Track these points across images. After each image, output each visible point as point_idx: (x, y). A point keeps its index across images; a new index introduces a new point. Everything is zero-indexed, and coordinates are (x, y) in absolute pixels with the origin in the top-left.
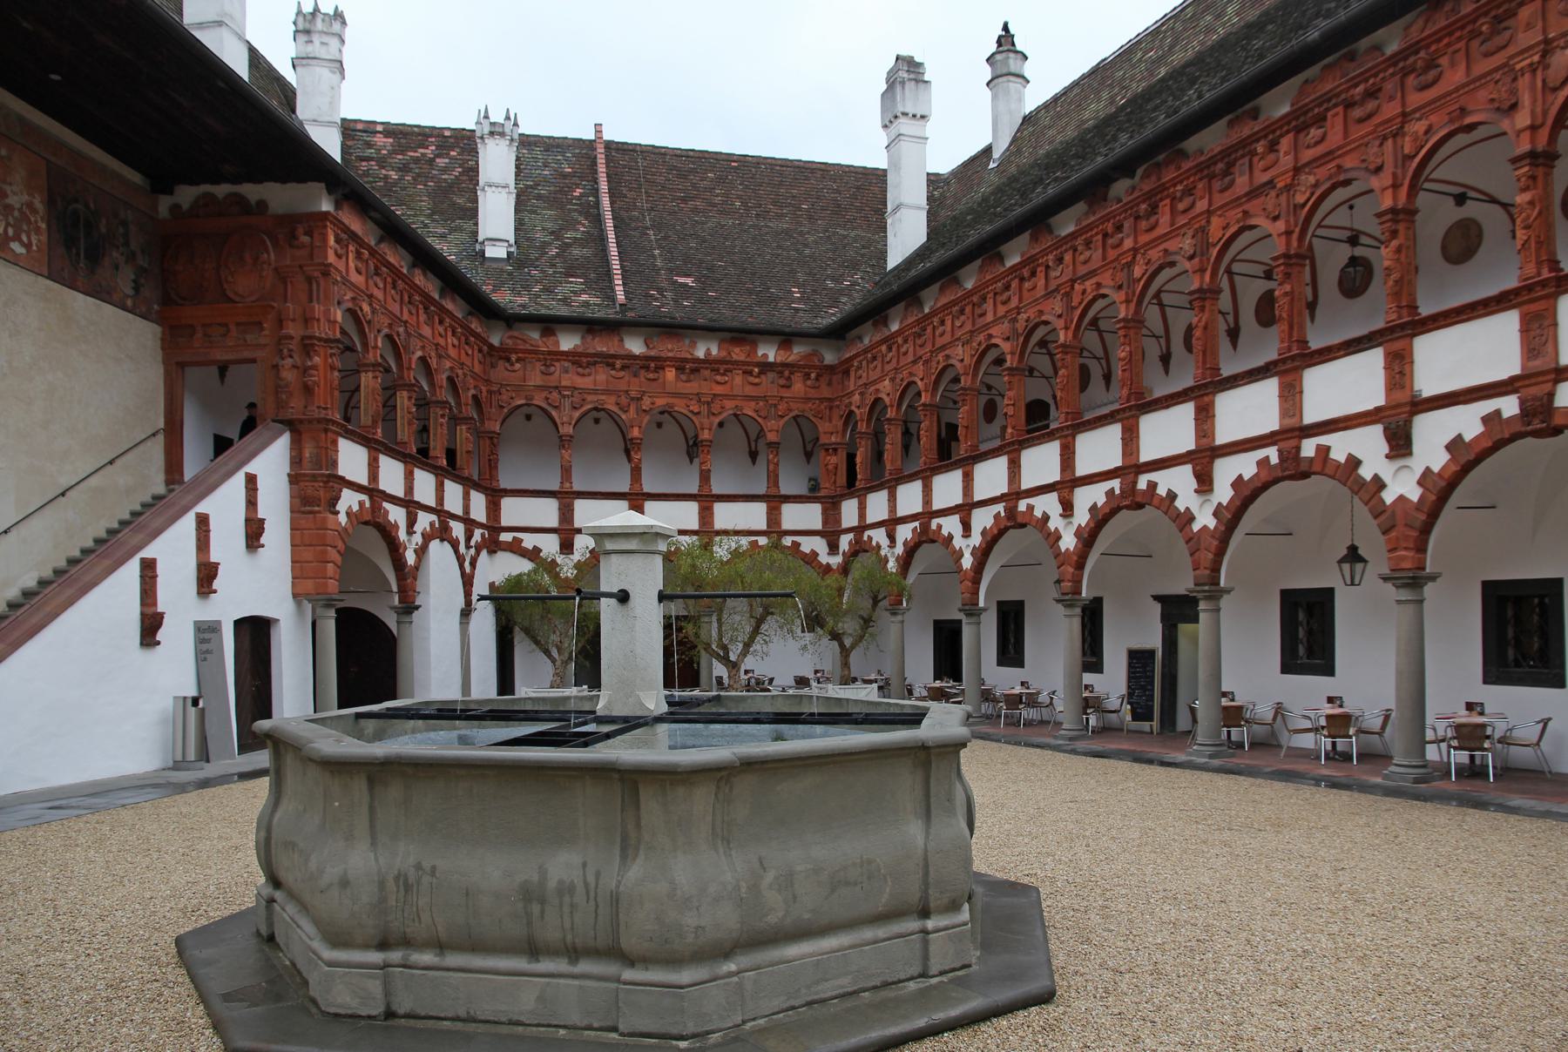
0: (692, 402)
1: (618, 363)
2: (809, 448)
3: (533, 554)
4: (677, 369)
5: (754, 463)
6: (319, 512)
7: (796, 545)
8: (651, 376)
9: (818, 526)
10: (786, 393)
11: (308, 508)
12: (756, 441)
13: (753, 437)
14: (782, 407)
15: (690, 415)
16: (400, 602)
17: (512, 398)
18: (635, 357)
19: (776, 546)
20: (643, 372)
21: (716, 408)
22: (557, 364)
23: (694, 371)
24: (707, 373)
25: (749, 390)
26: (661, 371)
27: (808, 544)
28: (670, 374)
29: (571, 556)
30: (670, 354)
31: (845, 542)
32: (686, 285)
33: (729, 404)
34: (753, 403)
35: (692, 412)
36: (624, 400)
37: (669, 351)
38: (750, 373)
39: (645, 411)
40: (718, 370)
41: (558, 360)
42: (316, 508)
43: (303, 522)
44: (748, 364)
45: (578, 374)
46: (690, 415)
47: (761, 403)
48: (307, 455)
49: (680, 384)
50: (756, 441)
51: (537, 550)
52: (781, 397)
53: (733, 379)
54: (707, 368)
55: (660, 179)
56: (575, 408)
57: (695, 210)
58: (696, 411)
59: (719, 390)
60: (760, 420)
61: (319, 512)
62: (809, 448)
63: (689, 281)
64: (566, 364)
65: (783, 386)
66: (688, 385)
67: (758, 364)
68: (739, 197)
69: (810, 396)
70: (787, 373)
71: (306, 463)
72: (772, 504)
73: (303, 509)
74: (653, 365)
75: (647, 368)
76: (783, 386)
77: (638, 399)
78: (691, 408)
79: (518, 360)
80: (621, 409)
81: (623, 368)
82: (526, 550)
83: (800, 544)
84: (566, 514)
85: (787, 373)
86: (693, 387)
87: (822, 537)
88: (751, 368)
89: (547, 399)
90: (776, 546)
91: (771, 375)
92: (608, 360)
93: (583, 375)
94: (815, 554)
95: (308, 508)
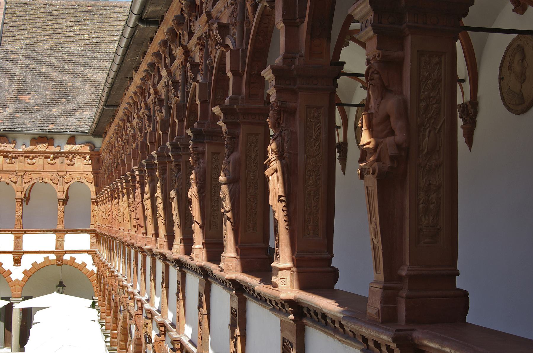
0: (12, 176)
4: (4, 157)
7: (73, 259)
9: (88, 248)
10: (69, 168)
14: (67, 177)
19: (60, 259)
21: (26, 178)
23: (16, 157)
25: (48, 168)
27: (80, 259)
32: (24, 102)
33: (34, 176)
34: (50, 175)
35: (12, 181)
38: (49, 158)
40: (29, 157)
44: (48, 153)
47: (55, 175)
49: (6, 165)
52: (67, 172)
53: (39, 162)
54: (22, 156)
58: (14, 181)
59: (29, 168)
63: (26, 98)
65: (69, 165)
69: (85, 170)
70: (71, 157)
76: (69, 165)
78: (12, 179)
83: (75, 259)
85: (71, 157)
87: (90, 254)
88: (49, 155)
90: (60, 259)
91: (61, 158)
94: (84, 264)
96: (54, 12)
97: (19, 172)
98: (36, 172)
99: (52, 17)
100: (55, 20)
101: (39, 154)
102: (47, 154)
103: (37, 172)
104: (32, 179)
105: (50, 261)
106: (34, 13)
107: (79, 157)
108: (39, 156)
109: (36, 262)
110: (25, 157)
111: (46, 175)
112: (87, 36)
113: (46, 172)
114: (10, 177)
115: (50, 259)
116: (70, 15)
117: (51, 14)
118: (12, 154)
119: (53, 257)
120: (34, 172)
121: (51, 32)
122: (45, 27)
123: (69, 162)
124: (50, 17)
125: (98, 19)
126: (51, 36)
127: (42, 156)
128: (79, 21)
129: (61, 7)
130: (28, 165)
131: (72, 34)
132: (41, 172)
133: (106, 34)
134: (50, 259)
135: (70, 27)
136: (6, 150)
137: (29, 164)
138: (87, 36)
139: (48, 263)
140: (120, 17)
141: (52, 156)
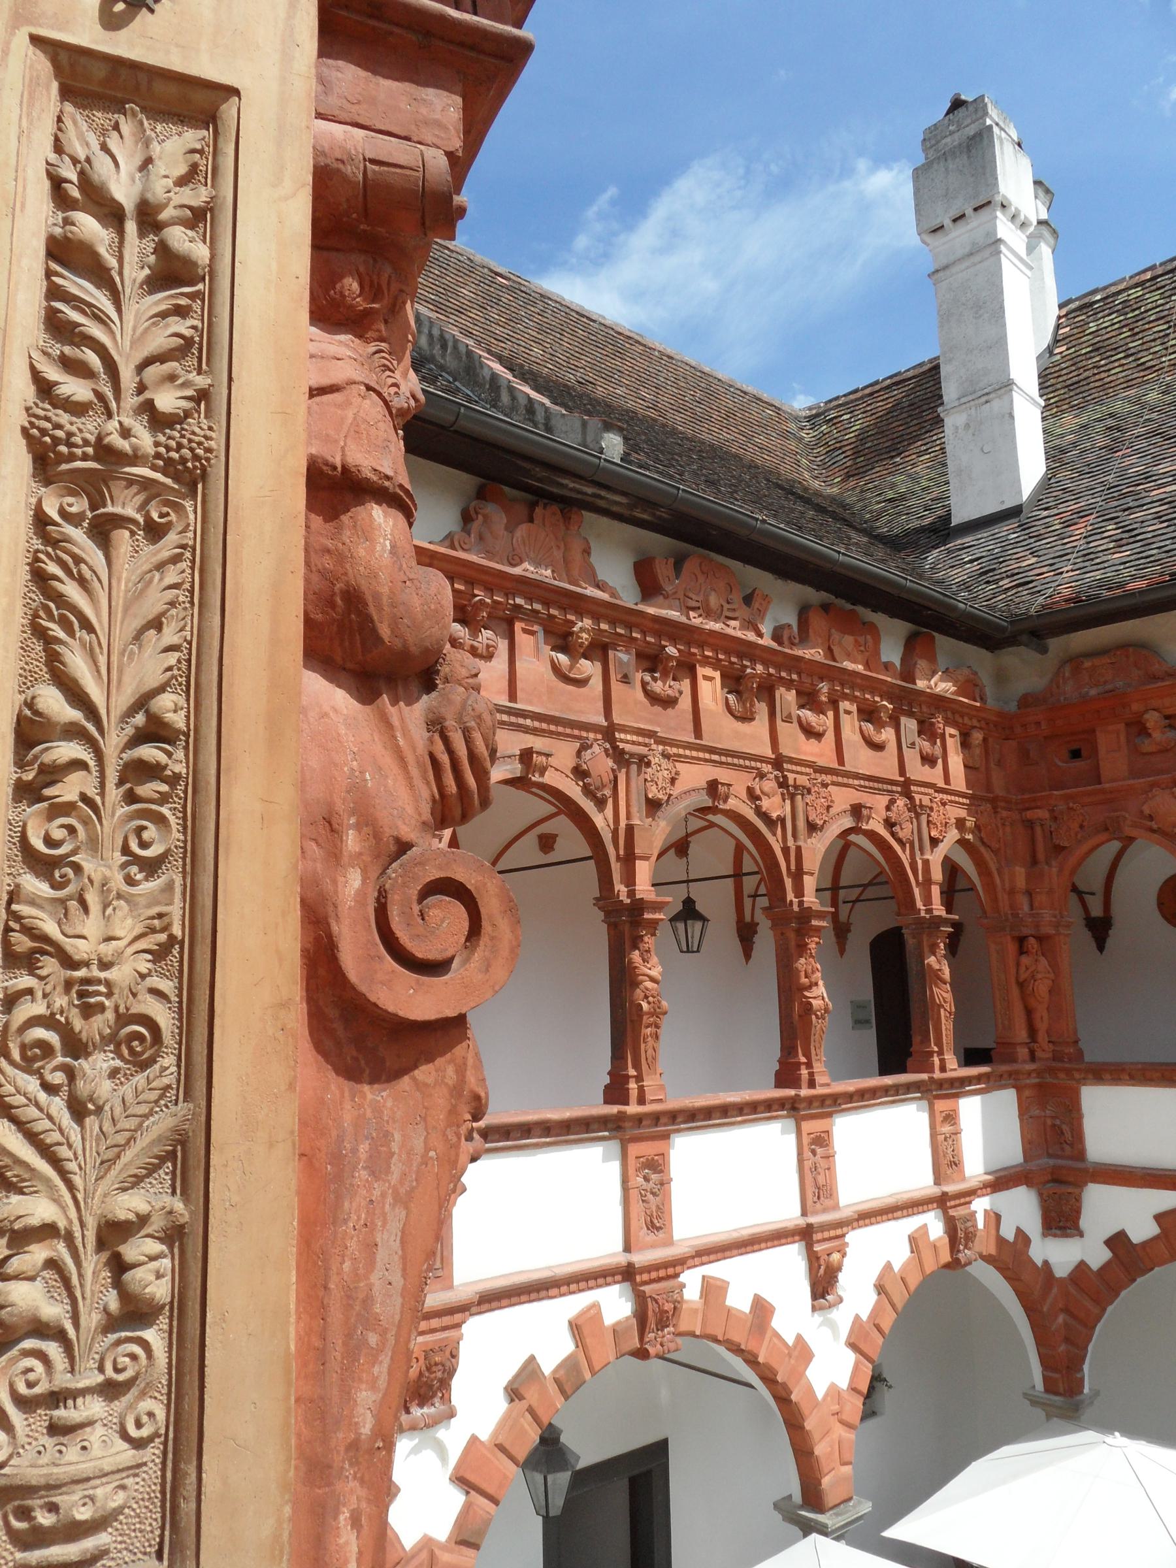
36: (600, 763)
78: (765, 804)
80: (587, 791)
81: (599, 650)
97: (794, 768)
113: (871, 784)
130: (802, 737)
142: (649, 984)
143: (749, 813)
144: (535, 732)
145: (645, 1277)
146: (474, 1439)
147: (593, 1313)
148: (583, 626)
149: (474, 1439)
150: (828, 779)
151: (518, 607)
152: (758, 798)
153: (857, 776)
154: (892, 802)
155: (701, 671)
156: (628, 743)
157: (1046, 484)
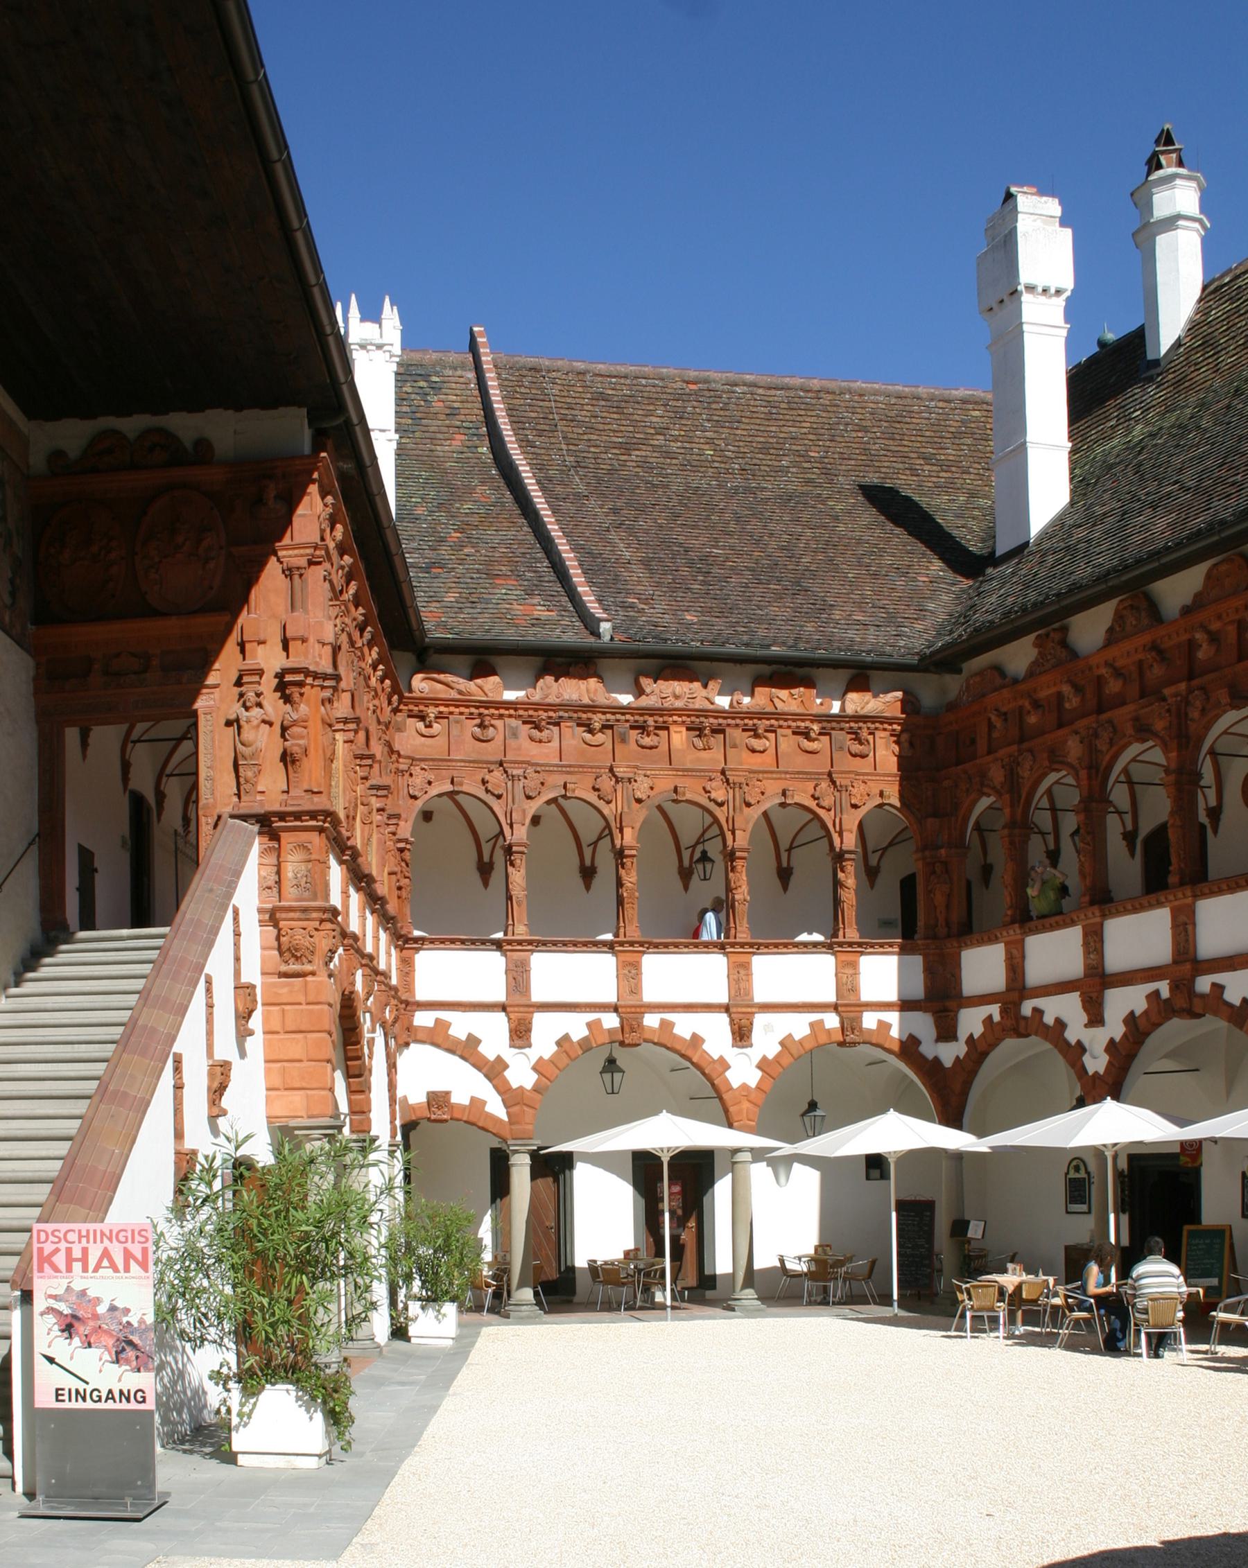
0: (714, 784)
1: (597, 720)
2: (873, 861)
3: (467, 1050)
4: (688, 729)
5: (588, 887)
6: (313, 974)
8: (647, 741)
11: (294, 967)
12: (789, 850)
13: (784, 844)
15: (712, 806)
16: (352, 1131)
17: (430, 783)
18: (624, 710)
20: (634, 734)
22: (498, 723)
24: (736, 734)
26: (663, 733)
28: (679, 737)
29: (526, 1050)
30: (679, 704)
31: (971, 1022)
36: (606, 783)
37: (677, 697)
38: (806, 734)
39: (639, 801)
41: (501, 716)
42: (308, 968)
43: (285, 990)
45: (532, 739)
46: (712, 806)
48: (290, 875)
50: (789, 850)
51: (473, 1041)
55: (581, 415)
56: (529, 797)
57: (644, 464)
58: (719, 800)
59: (755, 762)
60: (821, 812)
61: (313, 974)
62: (873, 861)
64: (514, 723)
66: (704, 754)
67: (818, 718)
68: (710, 442)
71: (290, 892)
72: (843, 957)
73: (284, 968)
74: (651, 721)
75: (642, 728)
77: (629, 780)
78: (713, 795)
79: (440, 717)
80: (600, 798)
82: (457, 1041)
84: (518, 978)
86: (713, 757)
89: (484, 782)
90: (850, 1024)
92: (582, 714)
93: (540, 741)
95: (294, 967)
96: (610, 392)
98: (774, 776)
99: (609, 404)
100: (619, 410)
101: (781, 723)
102: (803, 721)
103: (778, 776)
104: (763, 793)
105: (829, 1032)
106: (563, 394)
107: (883, 734)
108: (780, 727)
109: (790, 1035)
110: (744, 730)
111: (800, 785)
112: (712, 453)
114: (708, 788)
115: (828, 1026)
116: (652, 401)
117: (603, 396)
118: (712, 720)
119: (832, 1021)
120: (770, 775)
121: (620, 440)
122: (601, 427)
123: (856, 748)
124: (603, 403)
125: (722, 413)
126: (627, 448)
127: (789, 727)
128: (680, 415)
129: (622, 381)
131: (675, 446)
132: (788, 776)
133: (757, 451)
134: (828, 1026)
135: (661, 431)
136: (697, 707)
137: (753, 751)
138: (712, 453)
139: (823, 1039)
140: (774, 411)
141: (816, 727)
142: (629, 885)
143: (703, 800)
144: (568, 773)
145: (624, 1010)
146: (541, 1058)
147: (598, 1022)
148: (597, 720)
149: (541, 1058)
150: (760, 776)
151: (561, 717)
152: (709, 792)
153: (786, 773)
154: (816, 786)
155: (673, 728)
156: (619, 771)
157: (1059, 525)
